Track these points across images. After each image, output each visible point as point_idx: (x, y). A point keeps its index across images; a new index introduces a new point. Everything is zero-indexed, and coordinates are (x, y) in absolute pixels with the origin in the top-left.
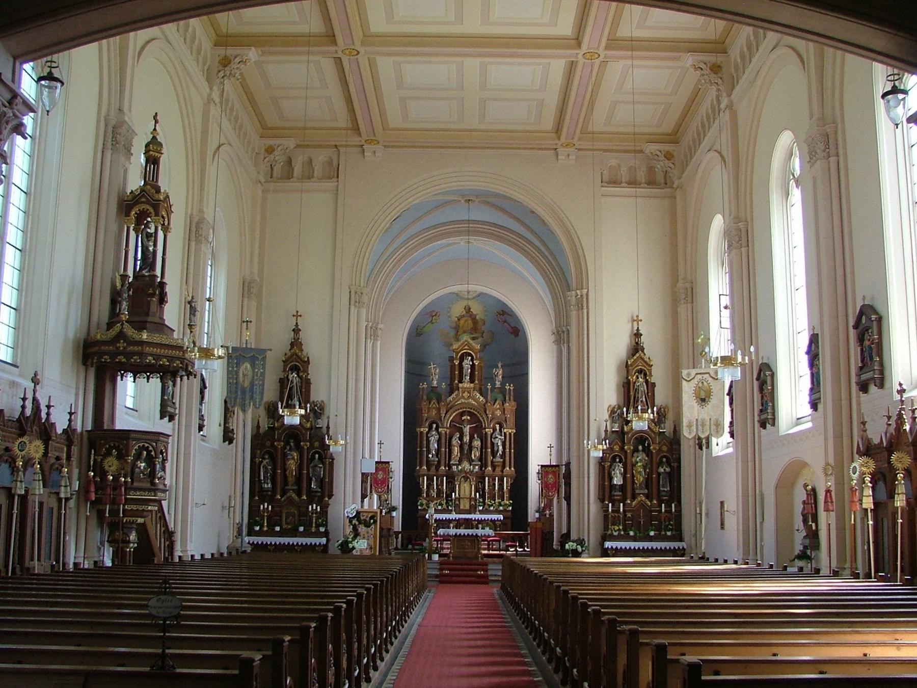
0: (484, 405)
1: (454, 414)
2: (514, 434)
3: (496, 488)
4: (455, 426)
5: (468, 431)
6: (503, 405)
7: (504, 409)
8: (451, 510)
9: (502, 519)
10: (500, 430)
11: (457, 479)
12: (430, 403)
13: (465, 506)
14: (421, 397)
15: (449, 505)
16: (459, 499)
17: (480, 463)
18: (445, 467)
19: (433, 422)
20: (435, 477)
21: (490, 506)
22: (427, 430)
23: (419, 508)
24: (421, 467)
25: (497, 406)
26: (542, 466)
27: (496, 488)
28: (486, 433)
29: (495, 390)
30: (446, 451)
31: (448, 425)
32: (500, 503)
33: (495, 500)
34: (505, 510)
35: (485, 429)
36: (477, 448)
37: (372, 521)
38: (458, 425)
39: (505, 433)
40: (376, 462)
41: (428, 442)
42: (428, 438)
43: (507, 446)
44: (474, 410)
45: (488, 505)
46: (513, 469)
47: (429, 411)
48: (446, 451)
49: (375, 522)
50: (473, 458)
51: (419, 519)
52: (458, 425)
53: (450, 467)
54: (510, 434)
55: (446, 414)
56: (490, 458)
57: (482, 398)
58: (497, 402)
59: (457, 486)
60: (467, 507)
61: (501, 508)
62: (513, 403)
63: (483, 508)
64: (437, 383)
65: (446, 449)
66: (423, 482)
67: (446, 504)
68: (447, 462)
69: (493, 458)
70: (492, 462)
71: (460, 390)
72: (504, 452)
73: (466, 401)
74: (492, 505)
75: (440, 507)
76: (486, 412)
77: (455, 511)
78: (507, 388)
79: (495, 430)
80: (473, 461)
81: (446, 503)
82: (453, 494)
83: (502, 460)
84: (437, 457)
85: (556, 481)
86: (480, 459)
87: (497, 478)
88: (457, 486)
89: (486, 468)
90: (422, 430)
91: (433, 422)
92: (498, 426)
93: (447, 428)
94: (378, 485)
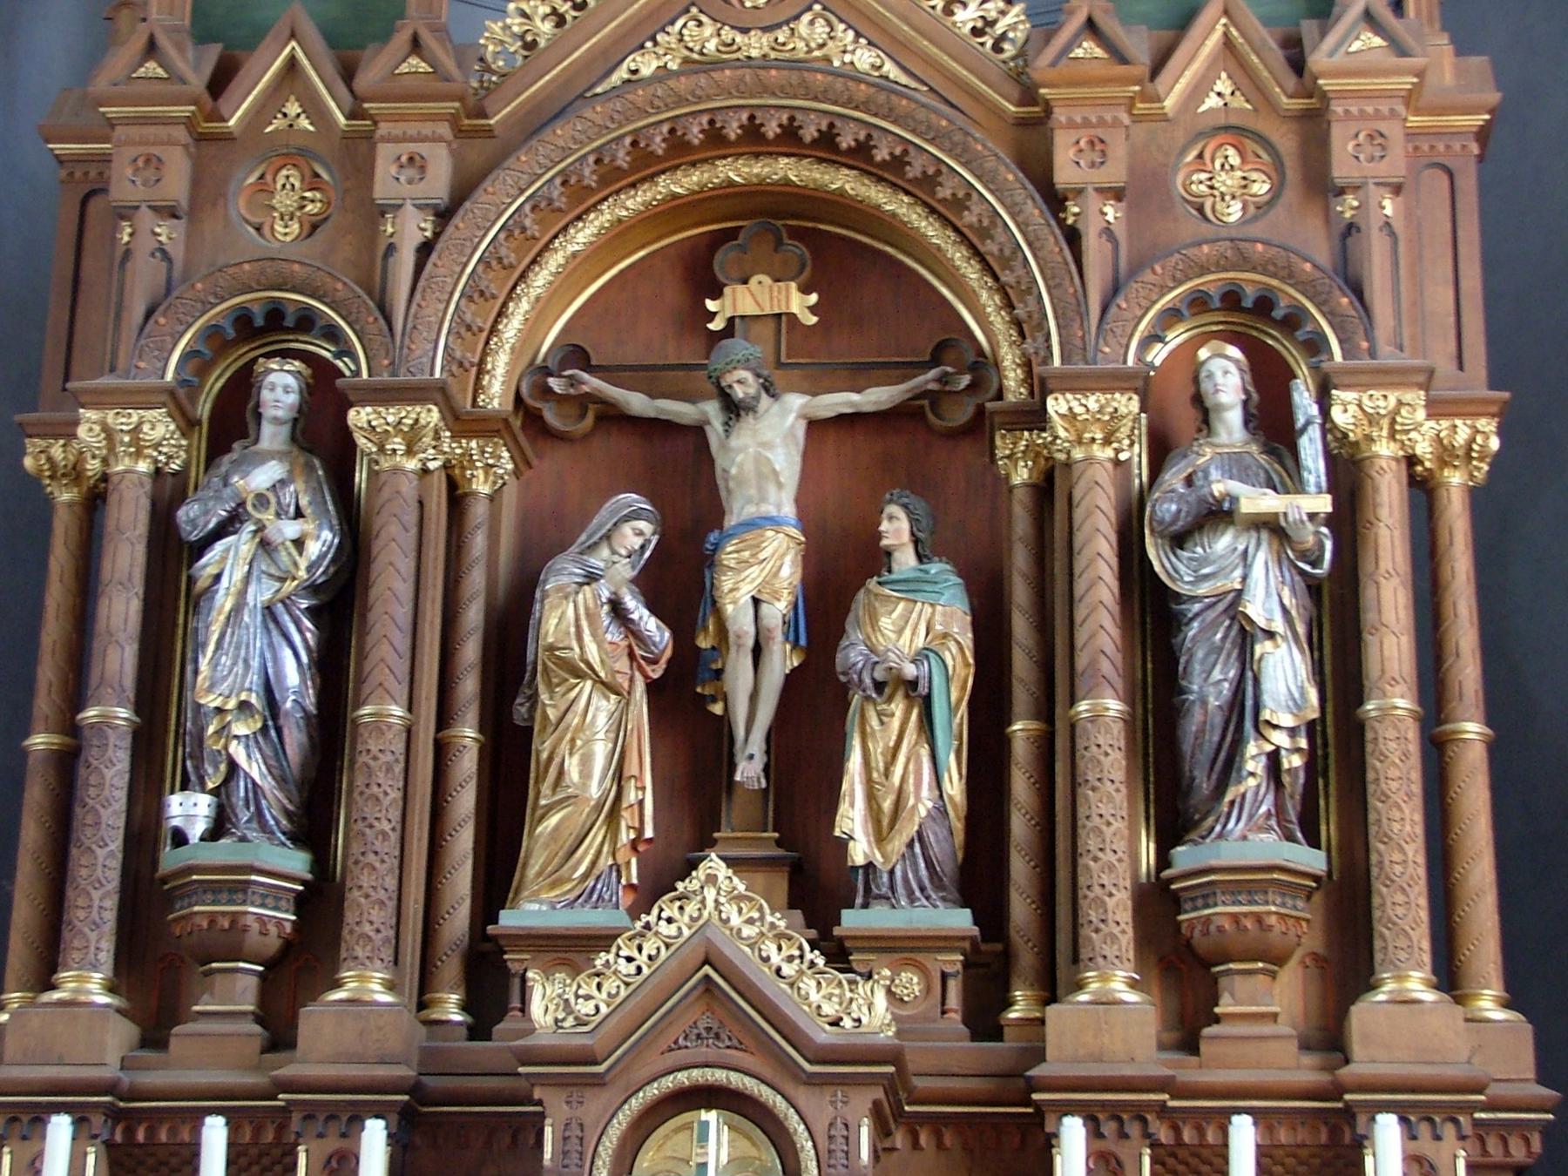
2: (1477, 497)
6: (1298, 64)
12: (221, 81)
17: (961, 920)
36: (918, 695)
38: (636, 402)
46: (1489, 1004)
48: (442, 752)
50: (859, 852)
55: (444, 216)
58: (1208, 37)
65: (444, 717)
68: (458, 920)
73: (755, 45)
83: (1313, 860)
93: (465, 423)
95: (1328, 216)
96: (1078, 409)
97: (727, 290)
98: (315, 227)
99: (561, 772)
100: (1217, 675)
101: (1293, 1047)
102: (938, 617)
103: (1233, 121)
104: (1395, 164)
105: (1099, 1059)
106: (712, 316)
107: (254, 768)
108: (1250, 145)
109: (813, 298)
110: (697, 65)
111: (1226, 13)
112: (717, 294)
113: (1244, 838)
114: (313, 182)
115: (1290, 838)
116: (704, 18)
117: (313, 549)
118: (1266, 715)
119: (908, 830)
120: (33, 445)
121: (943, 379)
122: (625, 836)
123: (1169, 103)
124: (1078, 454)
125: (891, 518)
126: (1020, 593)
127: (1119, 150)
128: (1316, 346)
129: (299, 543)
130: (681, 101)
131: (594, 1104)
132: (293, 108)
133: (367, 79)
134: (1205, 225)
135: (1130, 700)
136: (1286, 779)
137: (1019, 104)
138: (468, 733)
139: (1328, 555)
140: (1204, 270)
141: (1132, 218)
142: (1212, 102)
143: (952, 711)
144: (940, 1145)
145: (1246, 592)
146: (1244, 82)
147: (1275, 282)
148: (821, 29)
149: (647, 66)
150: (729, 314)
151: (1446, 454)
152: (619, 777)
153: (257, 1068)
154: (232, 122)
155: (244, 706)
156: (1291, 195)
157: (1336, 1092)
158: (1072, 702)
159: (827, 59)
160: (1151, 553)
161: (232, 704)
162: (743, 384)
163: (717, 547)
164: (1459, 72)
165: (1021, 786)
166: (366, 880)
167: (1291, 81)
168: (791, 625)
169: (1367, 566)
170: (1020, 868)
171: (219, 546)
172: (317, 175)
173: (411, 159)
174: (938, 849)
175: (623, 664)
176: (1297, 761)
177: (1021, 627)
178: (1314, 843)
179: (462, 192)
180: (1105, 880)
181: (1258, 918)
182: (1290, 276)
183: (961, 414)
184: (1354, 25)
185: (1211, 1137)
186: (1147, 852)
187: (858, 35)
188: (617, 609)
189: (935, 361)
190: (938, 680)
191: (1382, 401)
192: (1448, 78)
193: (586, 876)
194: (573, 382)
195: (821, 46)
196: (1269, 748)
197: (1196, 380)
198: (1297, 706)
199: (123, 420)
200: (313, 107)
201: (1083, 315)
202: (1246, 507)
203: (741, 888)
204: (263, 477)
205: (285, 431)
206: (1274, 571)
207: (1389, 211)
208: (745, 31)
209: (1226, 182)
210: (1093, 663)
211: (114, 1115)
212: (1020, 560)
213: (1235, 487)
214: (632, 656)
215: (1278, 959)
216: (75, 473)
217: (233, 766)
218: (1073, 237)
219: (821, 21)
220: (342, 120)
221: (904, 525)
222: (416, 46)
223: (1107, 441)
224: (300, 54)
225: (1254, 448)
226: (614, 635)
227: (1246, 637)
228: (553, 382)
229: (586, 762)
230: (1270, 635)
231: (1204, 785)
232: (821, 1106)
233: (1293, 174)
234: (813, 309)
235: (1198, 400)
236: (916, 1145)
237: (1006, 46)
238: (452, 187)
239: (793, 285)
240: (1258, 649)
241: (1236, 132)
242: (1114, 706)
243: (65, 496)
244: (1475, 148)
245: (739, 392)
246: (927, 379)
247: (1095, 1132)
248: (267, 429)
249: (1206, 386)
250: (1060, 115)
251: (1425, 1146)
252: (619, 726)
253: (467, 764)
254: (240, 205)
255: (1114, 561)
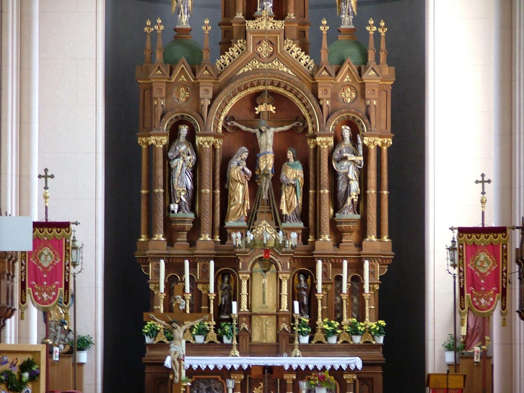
0: (312, 76)
1: (234, 101)
2: (389, 149)
3: (345, 289)
4: (238, 129)
5: (270, 141)
6: (360, 75)
7: (363, 85)
8: (229, 347)
9: (360, 366)
10: (354, 140)
11: (245, 267)
13: (263, 336)
14: (148, 54)
15: (224, 333)
16: (249, 317)
17: (301, 225)
18: (213, 236)
19: (181, 121)
20: (187, 263)
21: (327, 334)
22: (165, 140)
23: (148, 340)
24: (150, 235)
25: (344, 76)
26: (462, 231)
27: (345, 289)
28: (317, 148)
29: (340, 37)
30: (214, 195)
31: (220, 129)
32: (353, 326)
33: (340, 320)
34: (367, 346)
35: (314, 137)
37: (26, 375)
38: (244, 128)
39: (366, 149)
40: (36, 225)
41: (169, 171)
42: (167, 160)
43: (372, 181)
44: (285, 88)
45: (324, 330)
46: (385, 239)
47: (168, 94)
48: (214, 195)
49: (34, 377)
50: (285, 212)
51: (148, 370)
52: (244, 128)
53: (225, 235)
54: (379, 149)
56: (327, 210)
57: (305, 59)
58: (346, 68)
59: (244, 284)
60: (271, 337)
61: (357, 340)
62: (387, 71)
63: (311, 339)
64: (190, 21)
65: (214, 188)
66: (157, 273)
67: (216, 331)
69: (335, 212)
70: (333, 222)
71: (250, 37)
72: (363, 195)
73: (265, 66)
74: (334, 332)
75: (200, 339)
76: (315, 94)
77: (238, 349)
78: (371, 29)
79: (338, 140)
80: (283, 218)
81: (217, 327)
82: (234, 304)
83: (358, 217)
84: (192, 209)
85: (497, 269)
86: (303, 216)
87: (345, 263)
88: (244, 284)
89: (316, 237)
90: (152, 140)
91: (181, 121)
92: (347, 132)
93: (216, 136)
94: (41, 284)
95: (365, 103)
96: (322, 140)
97: (259, 106)
98: (188, 99)
99: (235, 199)
100: (344, 186)
101: (354, 247)
102: (298, 172)
103: (349, 84)
104: (376, 95)
105: (323, 250)
106: (256, 111)
107: (184, 199)
108: (352, 88)
109: (275, 108)
110: (255, 71)
111: (349, 64)
112: (257, 107)
113: (347, 214)
114: (187, 90)
115: (355, 213)
116: (257, 61)
117: (192, 161)
118: (351, 193)
119: (293, 209)
120: (139, 139)
121: (298, 124)
122: (245, 209)
123: (338, 81)
124: (322, 147)
125: (289, 153)
126: (311, 167)
127: (329, 92)
128: (363, 127)
129: (190, 160)
130: (253, 78)
131: (247, 260)
132: (183, 77)
133: (198, 76)
134: (344, 104)
135: (329, 190)
136: (354, 203)
137: (312, 80)
138: (218, 191)
139: (362, 165)
140: (343, 113)
141: (331, 103)
142: (346, 80)
143: (300, 188)
144: (298, 262)
145: (349, 173)
146: (351, 76)
147: (355, 116)
148: (277, 64)
149: (246, 70)
150: (259, 111)
151: (383, 144)
152: (244, 199)
153: (189, 250)
154: (173, 81)
155: (183, 190)
156: (359, 98)
157: (359, 255)
158: (320, 189)
159: (278, 69)
160: (334, 164)
161: (181, 189)
162: (263, 129)
163: (259, 156)
164: (389, 71)
165: (311, 201)
166: (205, 219)
167: (359, 78)
168: (272, 171)
169: (369, 167)
170: (311, 215)
171: (176, 160)
172: (187, 89)
173: (206, 90)
174: (297, 212)
175: (244, 179)
176: (356, 200)
177: (311, 174)
178: (359, 214)
179: (215, 95)
180: (325, 220)
181: (349, 227)
182: (358, 115)
183: (301, 130)
184: (371, 69)
185: (341, 261)
186: (332, 211)
187: (284, 64)
188: (243, 170)
189: (296, 120)
190: (298, 184)
191: (371, 139)
192: (387, 73)
193: (239, 216)
194: (232, 124)
195: (277, 67)
196: (352, 198)
197: (342, 132)
198: (356, 192)
199: (159, 139)
200: (186, 77)
201: (323, 122)
202: (349, 159)
203: (269, 226)
204: (183, 148)
205: (184, 138)
206: (354, 168)
207: (375, 103)
208: (263, 63)
209: (348, 95)
210: (324, 184)
211: (167, 258)
212: (311, 162)
213: (348, 155)
214: (245, 177)
215: (351, 232)
216: (147, 143)
217: (181, 199)
218: (321, 107)
219: (277, 62)
220: (192, 80)
221: (292, 154)
222: (206, 69)
223: (326, 145)
224: (184, 67)
225: (351, 145)
226: (242, 173)
227: (348, 180)
228: (229, 124)
229: (239, 197)
230: (352, 180)
231: (341, 204)
232: (282, 260)
233: (359, 95)
234: (275, 110)
235: (342, 135)
236: (295, 262)
237: (311, 69)
238: (213, 93)
239: (271, 105)
240: (350, 182)
241: (350, 86)
242: (327, 191)
243: (144, 147)
244: (391, 88)
245: (263, 130)
246: (295, 124)
247: (323, 261)
248: (181, 137)
249: (343, 134)
250: (319, 84)
251: (373, 263)
252: (244, 190)
253: (218, 197)
254: (174, 95)
255: (327, 166)
